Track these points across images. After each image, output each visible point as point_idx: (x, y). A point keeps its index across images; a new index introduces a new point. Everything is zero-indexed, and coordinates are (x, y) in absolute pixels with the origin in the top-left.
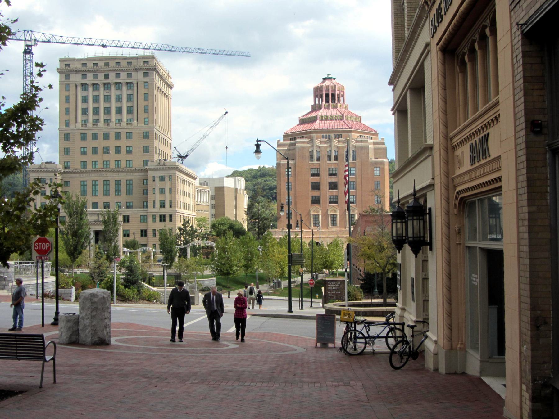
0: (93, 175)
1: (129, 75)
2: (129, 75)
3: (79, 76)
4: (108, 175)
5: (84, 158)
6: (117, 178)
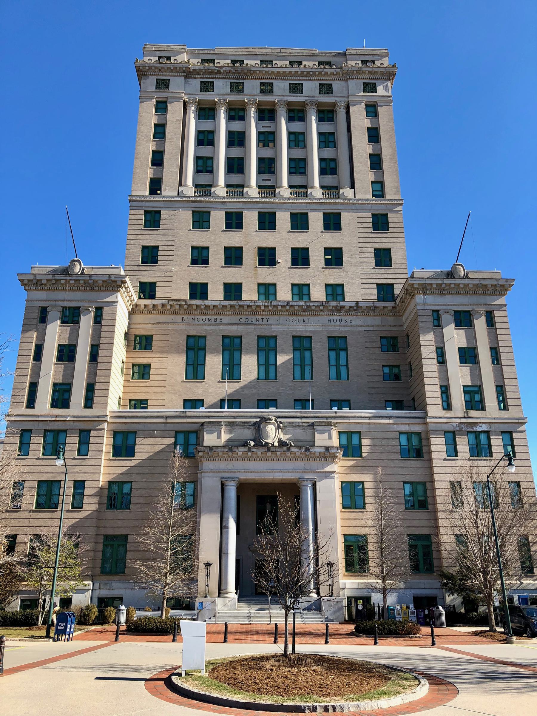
0: (226, 319)
1: (326, 89)
2: (326, 89)
3: (196, 84)
4: (273, 320)
6: (301, 329)
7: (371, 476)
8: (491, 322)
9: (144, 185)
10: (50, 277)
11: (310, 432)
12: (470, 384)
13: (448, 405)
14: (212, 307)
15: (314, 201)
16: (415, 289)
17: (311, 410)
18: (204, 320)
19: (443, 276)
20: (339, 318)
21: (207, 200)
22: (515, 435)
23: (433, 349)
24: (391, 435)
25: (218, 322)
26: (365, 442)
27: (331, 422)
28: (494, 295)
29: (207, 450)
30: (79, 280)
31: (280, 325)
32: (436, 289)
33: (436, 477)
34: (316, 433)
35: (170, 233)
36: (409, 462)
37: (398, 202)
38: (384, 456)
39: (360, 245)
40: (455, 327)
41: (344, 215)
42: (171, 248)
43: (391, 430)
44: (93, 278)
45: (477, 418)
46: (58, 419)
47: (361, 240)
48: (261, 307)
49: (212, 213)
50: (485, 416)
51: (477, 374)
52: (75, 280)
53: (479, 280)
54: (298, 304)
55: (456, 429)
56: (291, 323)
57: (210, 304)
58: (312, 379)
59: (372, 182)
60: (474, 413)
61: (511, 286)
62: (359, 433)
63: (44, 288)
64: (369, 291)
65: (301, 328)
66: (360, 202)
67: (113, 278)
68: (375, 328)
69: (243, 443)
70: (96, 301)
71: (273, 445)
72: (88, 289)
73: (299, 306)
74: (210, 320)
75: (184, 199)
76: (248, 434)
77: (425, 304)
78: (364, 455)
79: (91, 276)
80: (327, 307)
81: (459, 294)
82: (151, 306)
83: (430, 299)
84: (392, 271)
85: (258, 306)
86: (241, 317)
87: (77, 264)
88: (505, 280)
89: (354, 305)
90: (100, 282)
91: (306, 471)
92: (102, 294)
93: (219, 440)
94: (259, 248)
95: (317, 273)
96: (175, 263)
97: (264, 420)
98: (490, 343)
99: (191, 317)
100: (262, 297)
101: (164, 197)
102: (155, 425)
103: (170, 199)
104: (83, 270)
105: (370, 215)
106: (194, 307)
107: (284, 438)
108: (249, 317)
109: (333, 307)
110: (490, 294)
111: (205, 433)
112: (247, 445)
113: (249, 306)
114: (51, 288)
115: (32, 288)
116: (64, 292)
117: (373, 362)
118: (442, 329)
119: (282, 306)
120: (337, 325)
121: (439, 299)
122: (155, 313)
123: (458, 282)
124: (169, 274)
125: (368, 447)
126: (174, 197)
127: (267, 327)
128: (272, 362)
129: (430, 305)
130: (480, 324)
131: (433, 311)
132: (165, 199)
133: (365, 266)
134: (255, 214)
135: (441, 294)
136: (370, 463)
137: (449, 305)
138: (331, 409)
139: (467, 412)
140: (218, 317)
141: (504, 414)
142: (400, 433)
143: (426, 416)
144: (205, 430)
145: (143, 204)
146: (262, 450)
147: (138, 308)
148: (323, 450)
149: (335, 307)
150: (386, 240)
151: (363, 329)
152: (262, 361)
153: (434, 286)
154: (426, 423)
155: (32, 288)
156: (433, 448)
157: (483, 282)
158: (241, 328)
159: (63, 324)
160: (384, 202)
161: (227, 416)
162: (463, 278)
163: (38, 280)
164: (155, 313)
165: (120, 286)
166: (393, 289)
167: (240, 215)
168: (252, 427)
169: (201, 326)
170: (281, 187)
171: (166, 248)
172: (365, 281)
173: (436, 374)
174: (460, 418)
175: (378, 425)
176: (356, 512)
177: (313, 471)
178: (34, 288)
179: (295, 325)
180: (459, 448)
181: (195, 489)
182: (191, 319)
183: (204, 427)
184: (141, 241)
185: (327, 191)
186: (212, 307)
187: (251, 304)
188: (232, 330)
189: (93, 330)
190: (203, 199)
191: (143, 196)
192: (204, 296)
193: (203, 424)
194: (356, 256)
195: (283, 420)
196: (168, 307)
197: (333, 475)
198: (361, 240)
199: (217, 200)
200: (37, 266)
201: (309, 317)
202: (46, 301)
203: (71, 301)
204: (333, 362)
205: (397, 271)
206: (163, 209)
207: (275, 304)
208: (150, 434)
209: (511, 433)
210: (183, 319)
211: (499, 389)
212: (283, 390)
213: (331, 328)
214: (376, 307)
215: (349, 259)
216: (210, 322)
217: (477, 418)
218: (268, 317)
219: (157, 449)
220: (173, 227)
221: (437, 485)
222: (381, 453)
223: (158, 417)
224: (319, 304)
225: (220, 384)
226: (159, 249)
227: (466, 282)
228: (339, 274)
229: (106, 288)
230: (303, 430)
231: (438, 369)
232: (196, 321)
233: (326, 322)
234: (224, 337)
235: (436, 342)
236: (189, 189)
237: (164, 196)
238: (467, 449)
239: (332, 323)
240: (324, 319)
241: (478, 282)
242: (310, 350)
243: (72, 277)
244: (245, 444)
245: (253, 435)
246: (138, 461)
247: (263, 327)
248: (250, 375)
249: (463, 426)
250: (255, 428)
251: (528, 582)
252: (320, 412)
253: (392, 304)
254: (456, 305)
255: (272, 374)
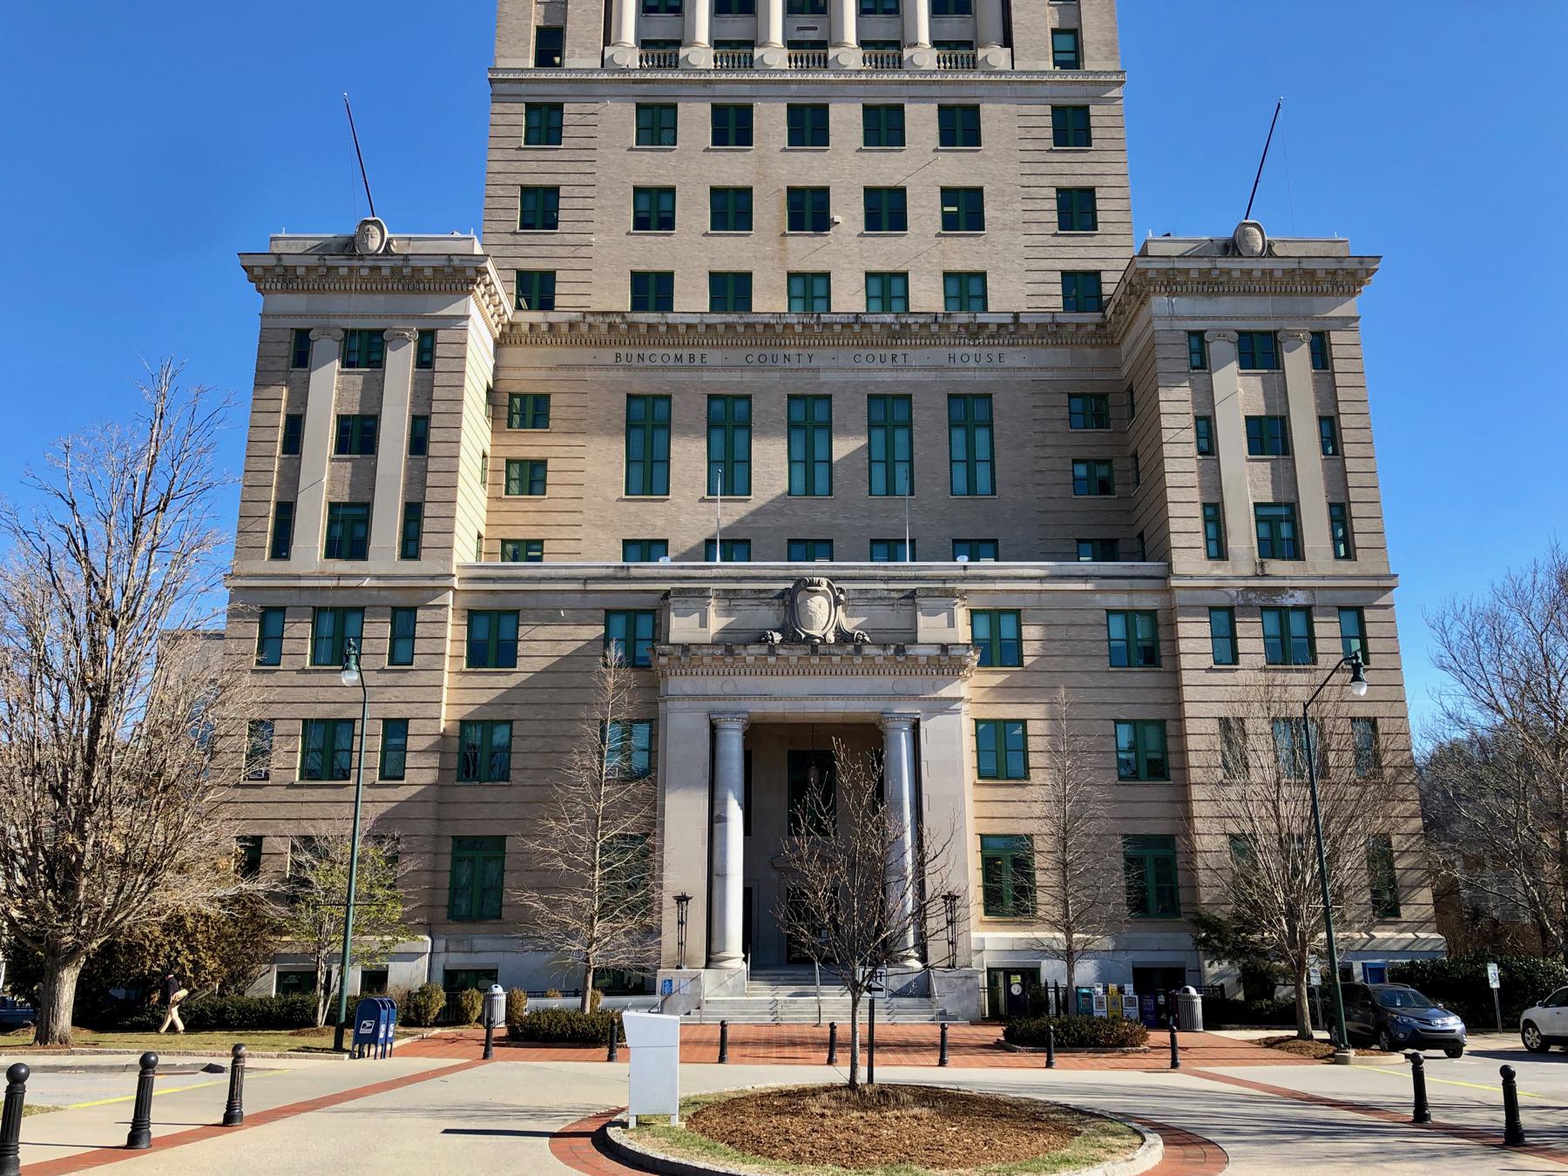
0: (715, 357)
4: (822, 357)
5: (653, 252)
6: (886, 379)
7: (1043, 708)
8: (1321, 357)
9: (522, 44)
10: (313, 260)
11: (907, 611)
12: (1271, 500)
13: (1218, 548)
14: (682, 329)
15: (918, 78)
16: (1151, 282)
17: (908, 563)
18: (666, 358)
19: (1215, 252)
20: (973, 351)
21: (670, 76)
22: (1368, 615)
23: (1189, 420)
24: (1090, 617)
25: (698, 362)
26: (1029, 632)
27: (953, 589)
28: (1332, 294)
29: (678, 652)
30: (380, 268)
31: (838, 369)
32: (1198, 283)
33: (1189, 710)
34: (919, 613)
35: (585, 155)
36: (1127, 675)
37: (1114, 78)
38: (1072, 663)
39: (1025, 181)
40: (1240, 371)
41: (987, 110)
42: (587, 191)
43: (1091, 605)
44: (412, 263)
45: (1284, 578)
46: (343, 583)
47: (1027, 169)
48: (796, 327)
49: (682, 108)
50: (1302, 573)
51: (1286, 478)
52: (372, 269)
53: (1297, 260)
54: (880, 320)
55: (1235, 603)
56: (864, 364)
57: (678, 321)
58: (912, 493)
59: (1054, 31)
60: (1276, 567)
61: (1370, 272)
62: (1017, 612)
63: (300, 287)
64: (1043, 289)
65: (887, 376)
66: (1024, 78)
67: (456, 261)
68: (1055, 375)
69: (757, 636)
70: (420, 317)
71: (823, 640)
72: (400, 287)
73: (883, 325)
74: (679, 358)
75: (616, 76)
76: (767, 616)
77: (1173, 317)
78: (1027, 661)
79: (406, 257)
80: (948, 326)
81: (1249, 293)
82: (544, 328)
83: (1183, 305)
84: (1097, 240)
85: (786, 326)
86: (749, 351)
87: (375, 230)
88: (1357, 259)
89: (1010, 320)
90: (428, 272)
91: (897, 696)
92: (432, 299)
93: (704, 630)
94: (791, 190)
95: (923, 247)
96: (598, 226)
97: (804, 586)
98: (1318, 406)
99: (635, 352)
100: (799, 305)
101: (570, 70)
102: (560, 597)
103: (584, 77)
104: (388, 244)
105: (1049, 110)
106: (643, 329)
107: (848, 624)
108: (768, 352)
109: (960, 325)
110: (1327, 294)
111: (672, 614)
112: (767, 640)
113: (767, 326)
114: (316, 287)
115: (273, 287)
116: (346, 296)
117: (1050, 451)
118: (1210, 374)
119: (844, 325)
120: (968, 369)
121: (1204, 306)
122: (554, 342)
123: (1247, 264)
124: (583, 251)
125: (1037, 644)
126: (592, 71)
127: (810, 374)
128: (820, 454)
129: (1183, 318)
130: (1297, 361)
131: (1191, 333)
132: (573, 76)
133: (1034, 229)
134: (782, 109)
135: (1209, 295)
136: (1042, 680)
137: (1226, 319)
138: (955, 560)
139: (1262, 564)
140: (697, 352)
141: (1346, 567)
142: (1110, 612)
143: (1168, 573)
144: (672, 607)
145: (523, 88)
146: (800, 651)
147: (514, 332)
148: (935, 651)
149: (966, 326)
150: (1085, 169)
151: (1030, 375)
152: (799, 454)
153: (1194, 274)
154: (1169, 590)
155: (273, 287)
156: (1184, 646)
157: (1306, 265)
158: (748, 376)
159: (347, 370)
160: (1080, 78)
161: (721, 578)
162: (1260, 256)
163: (286, 269)
164: (554, 342)
165: (473, 282)
166: (1099, 283)
167: (745, 113)
168: (776, 601)
169: (659, 374)
170: (840, 44)
171: (577, 191)
172: (1035, 265)
173: (1193, 479)
174: (1246, 578)
175: (1060, 595)
176: (1008, 785)
177: (912, 696)
178: (279, 286)
179: (874, 370)
180: (1243, 645)
181: (653, 736)
182: (635, 357)
183: (671, 600)
184: (518, 176)
185: (947, 53)
186: (682, 329)
187: (773, 321)
188: (730, 382)
189: (416, 383)
190: (659, 76)
191: (522, 70)
192: (665, 304)
193: (667, 595)
194: (1015, 206)
195: (845, 586)
196: (584, 328)
197: (957, 706)
198: (1027, 169)
199: (692, 77)
200: (283, 235)
201: (905, 351)
202: (306, 316)
203: (363, 317)
204: (960, 454)
205: (1109, 240)
206: (569, 99)
207: (827, 321)
208: (550, 617)
209: (1359, 611)
210: (618, 356)
211: (1336, 512)
212: (846, 518)
213: (955, 375)
214: (1059, 325)
215: (997, 214)
216: (680, 363)
217: (1284, 578)
218: (810, 351)
219: (567, 649)
220: (592, 143)
221: (1191, 726)
222: (1066, 656)
223: (567, 579)
224: (929, 321)
225: (704, 504)
226: (561, 194)
227: (1268, 264)
228: (975, 249)
229: (443, 286)
230: (891, 608)
231: (1199, 468)
232: (647, 362)
233: (944, 361)
234: (711, 397)
235: (1195, 405)
236: (627, 53)
237: (570, 70)
238: (1259, 646)
239: (959, 363)
240: (939, 354)
241: (1295, 266)
242: (908, 425)
243: (363, 259)
244: (761, 639)
245: (778, 619)
246: (524, 677)
247: (798, 374)
248: (772, 486)
249: (1252, 595)
250: (784, 604)
251: (1387, 935)
252: (930, 568)
253: (1095, 317)
254: (1243, 318)
255: (821, 483)
